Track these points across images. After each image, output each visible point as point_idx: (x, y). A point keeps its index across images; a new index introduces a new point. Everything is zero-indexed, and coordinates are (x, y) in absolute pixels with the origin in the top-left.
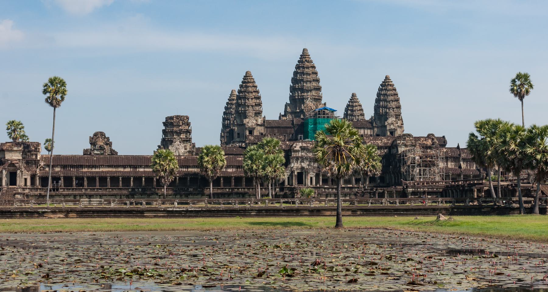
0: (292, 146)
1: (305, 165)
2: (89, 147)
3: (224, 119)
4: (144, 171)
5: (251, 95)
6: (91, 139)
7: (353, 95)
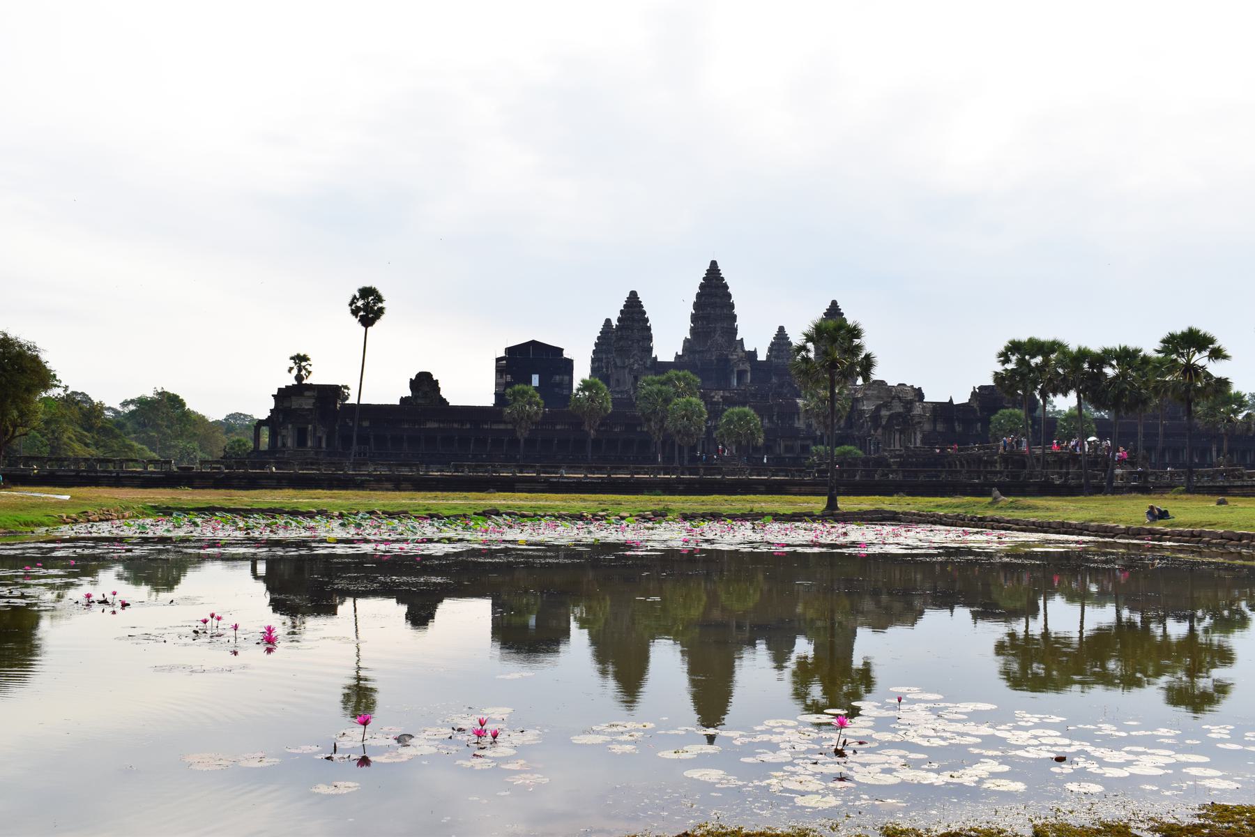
2: (408, 393)
3: (593, 361)
5: (636, 325)
7: (781, 329)
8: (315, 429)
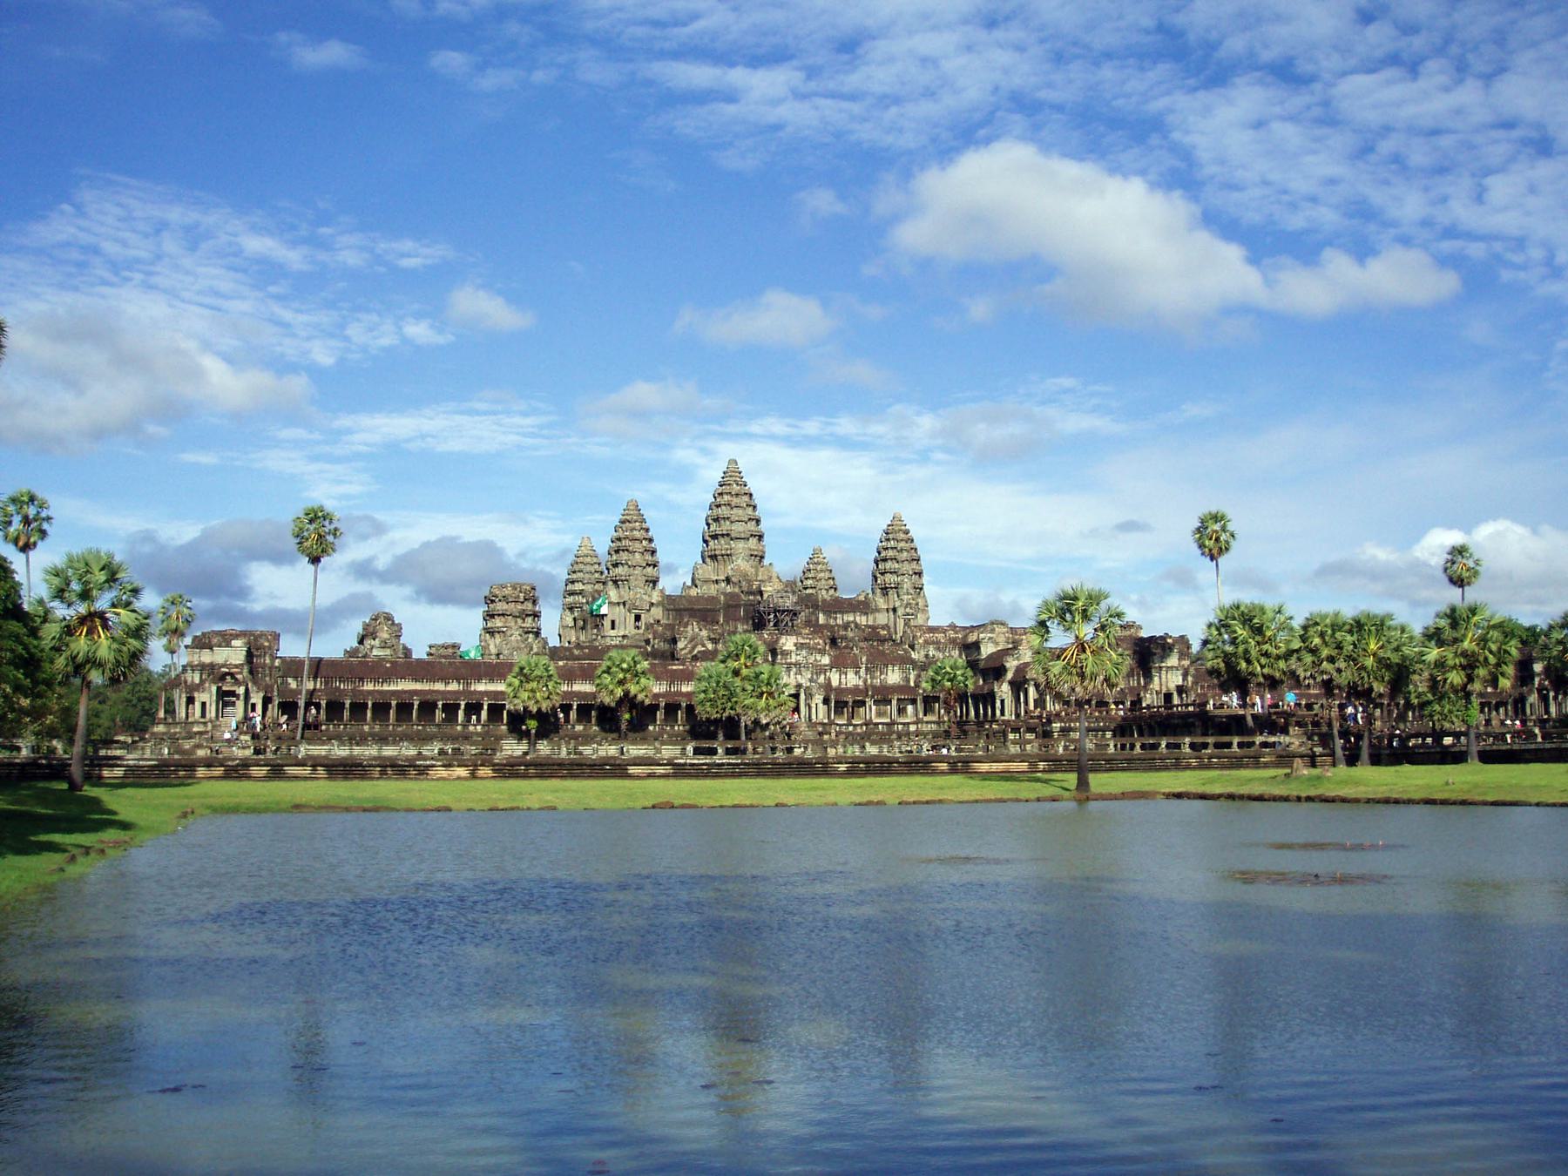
0: (777, 641)
1: (804, 681)
4: (486, 693)
5: (637, 544)
6: (366, 626)
8: (247, 690)
